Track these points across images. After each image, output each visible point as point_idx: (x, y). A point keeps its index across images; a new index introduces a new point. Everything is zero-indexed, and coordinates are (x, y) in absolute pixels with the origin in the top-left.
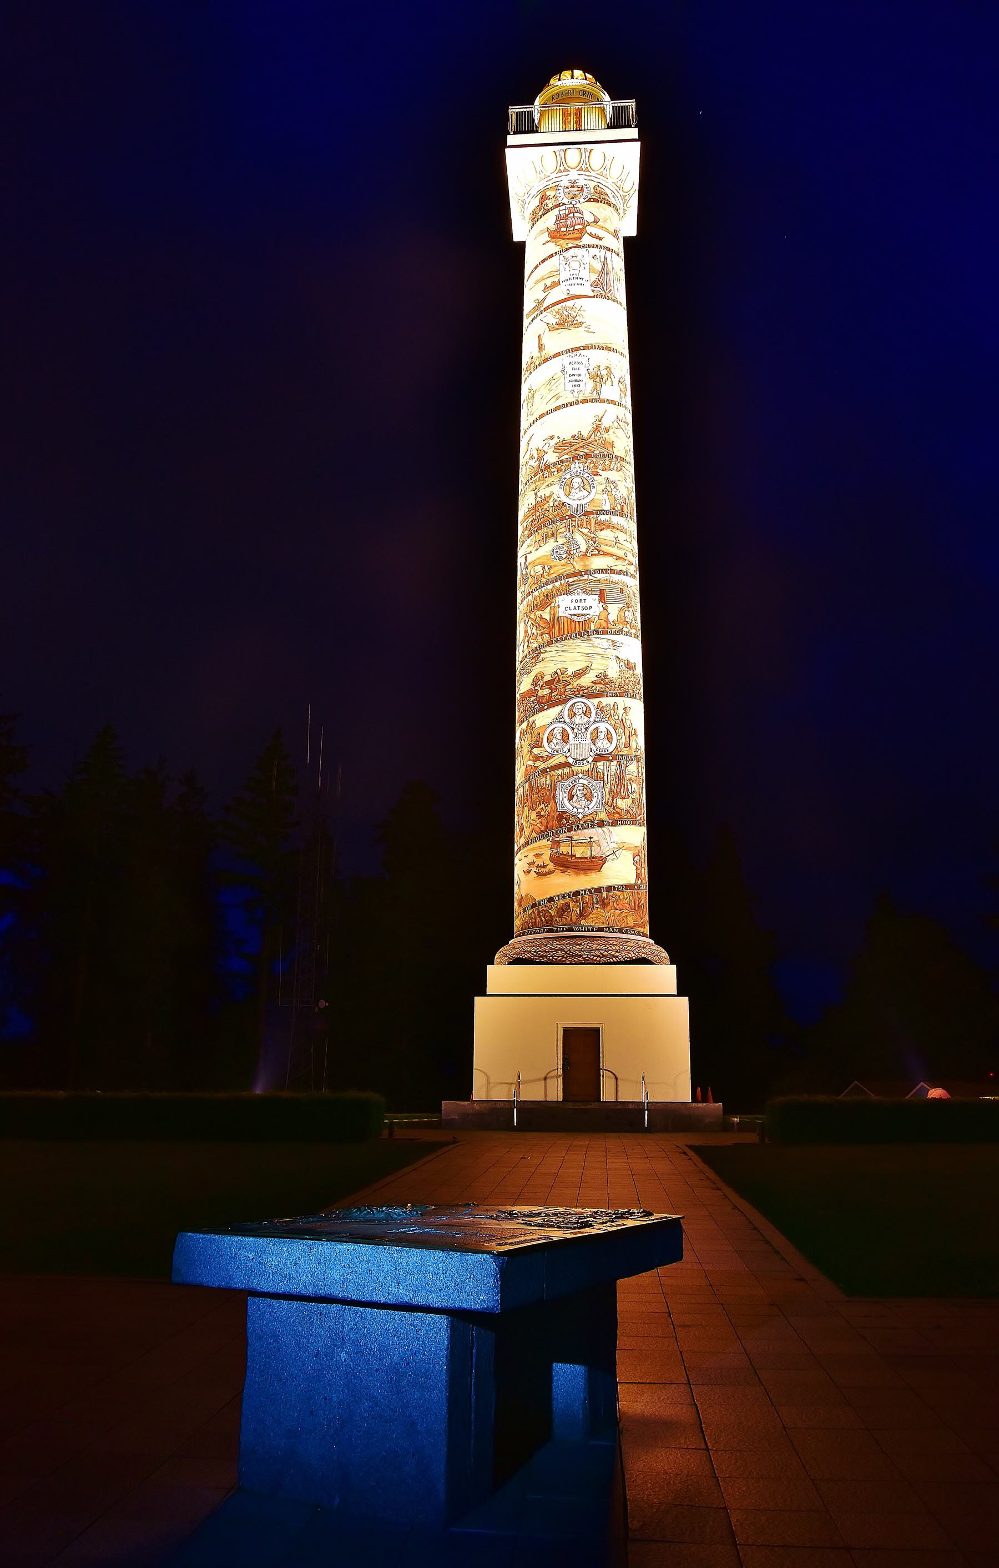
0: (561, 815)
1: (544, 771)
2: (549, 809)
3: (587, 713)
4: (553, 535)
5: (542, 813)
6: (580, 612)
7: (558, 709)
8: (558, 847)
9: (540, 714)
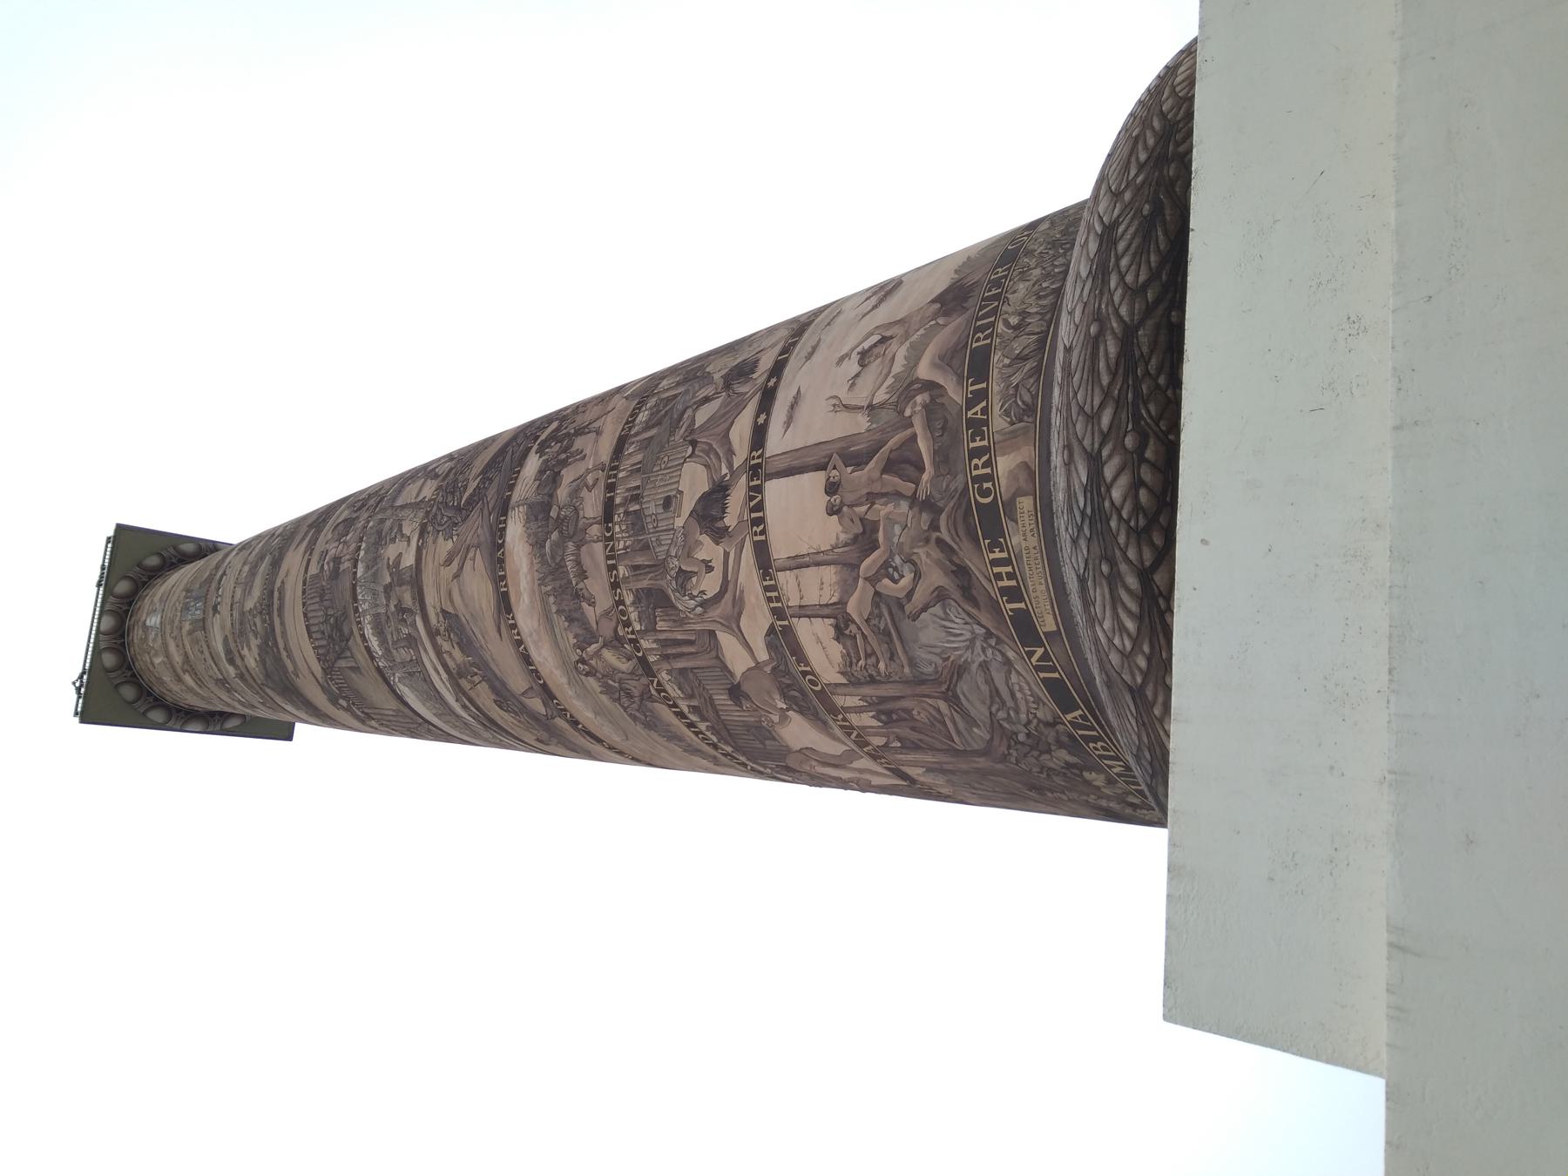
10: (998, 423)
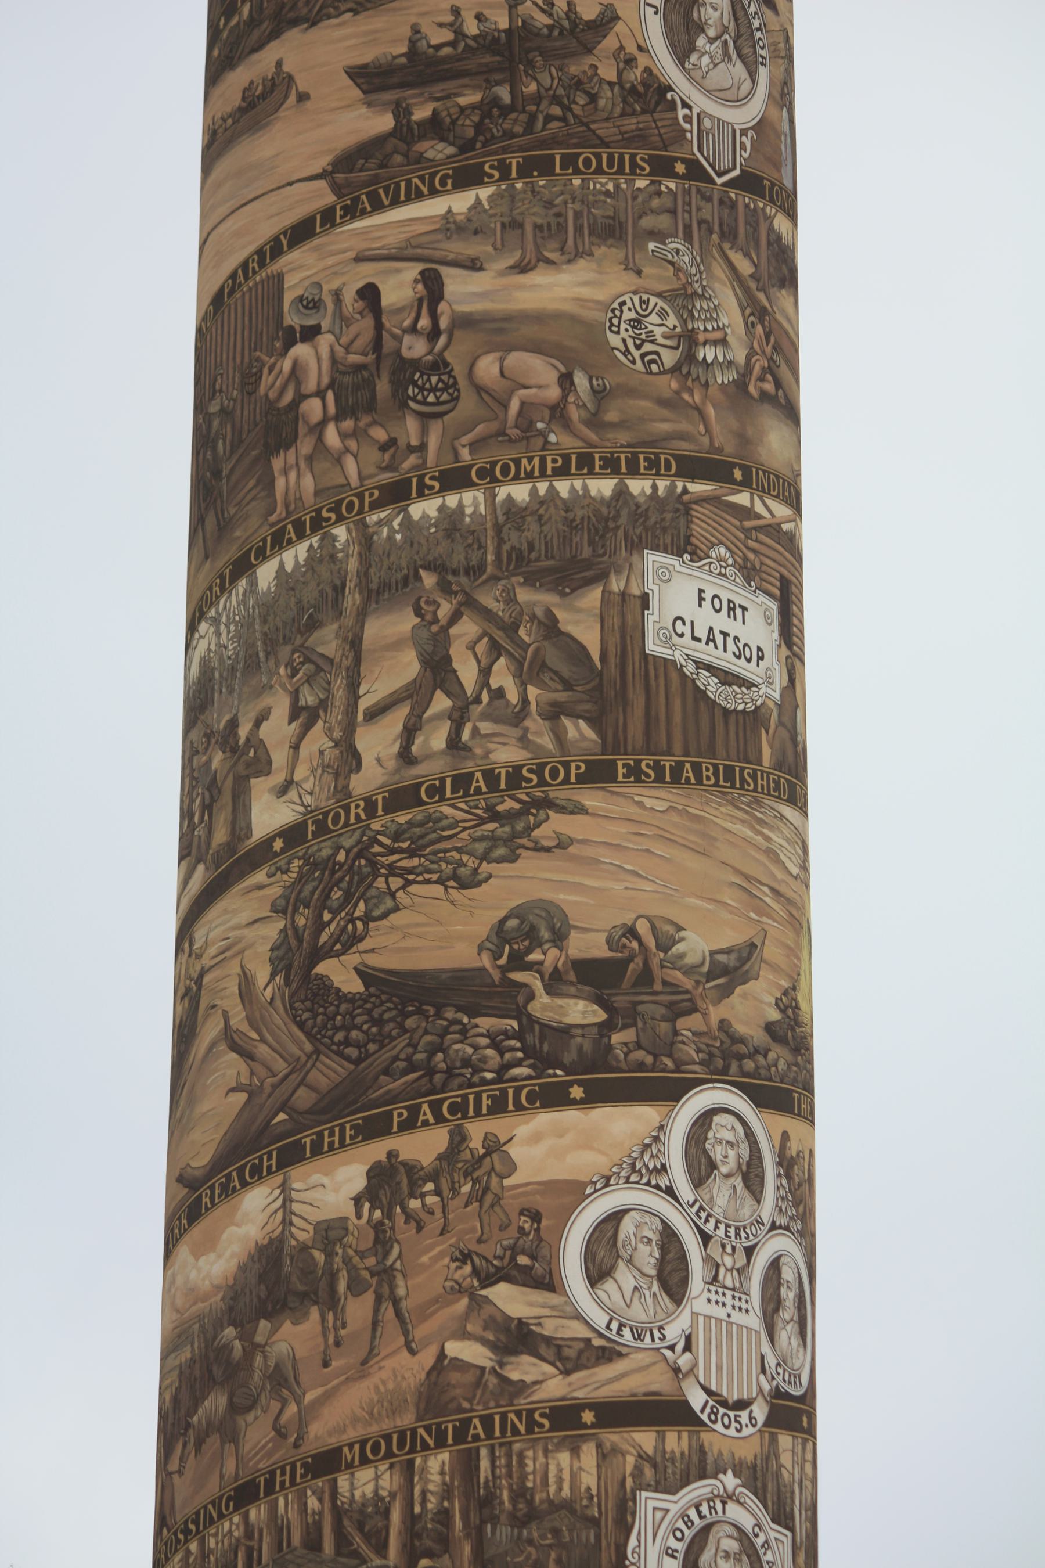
1: (565, 1416)
3: (751, 1177)
4: (612, 231)
6: (725, 660)
9: (545, 1119)
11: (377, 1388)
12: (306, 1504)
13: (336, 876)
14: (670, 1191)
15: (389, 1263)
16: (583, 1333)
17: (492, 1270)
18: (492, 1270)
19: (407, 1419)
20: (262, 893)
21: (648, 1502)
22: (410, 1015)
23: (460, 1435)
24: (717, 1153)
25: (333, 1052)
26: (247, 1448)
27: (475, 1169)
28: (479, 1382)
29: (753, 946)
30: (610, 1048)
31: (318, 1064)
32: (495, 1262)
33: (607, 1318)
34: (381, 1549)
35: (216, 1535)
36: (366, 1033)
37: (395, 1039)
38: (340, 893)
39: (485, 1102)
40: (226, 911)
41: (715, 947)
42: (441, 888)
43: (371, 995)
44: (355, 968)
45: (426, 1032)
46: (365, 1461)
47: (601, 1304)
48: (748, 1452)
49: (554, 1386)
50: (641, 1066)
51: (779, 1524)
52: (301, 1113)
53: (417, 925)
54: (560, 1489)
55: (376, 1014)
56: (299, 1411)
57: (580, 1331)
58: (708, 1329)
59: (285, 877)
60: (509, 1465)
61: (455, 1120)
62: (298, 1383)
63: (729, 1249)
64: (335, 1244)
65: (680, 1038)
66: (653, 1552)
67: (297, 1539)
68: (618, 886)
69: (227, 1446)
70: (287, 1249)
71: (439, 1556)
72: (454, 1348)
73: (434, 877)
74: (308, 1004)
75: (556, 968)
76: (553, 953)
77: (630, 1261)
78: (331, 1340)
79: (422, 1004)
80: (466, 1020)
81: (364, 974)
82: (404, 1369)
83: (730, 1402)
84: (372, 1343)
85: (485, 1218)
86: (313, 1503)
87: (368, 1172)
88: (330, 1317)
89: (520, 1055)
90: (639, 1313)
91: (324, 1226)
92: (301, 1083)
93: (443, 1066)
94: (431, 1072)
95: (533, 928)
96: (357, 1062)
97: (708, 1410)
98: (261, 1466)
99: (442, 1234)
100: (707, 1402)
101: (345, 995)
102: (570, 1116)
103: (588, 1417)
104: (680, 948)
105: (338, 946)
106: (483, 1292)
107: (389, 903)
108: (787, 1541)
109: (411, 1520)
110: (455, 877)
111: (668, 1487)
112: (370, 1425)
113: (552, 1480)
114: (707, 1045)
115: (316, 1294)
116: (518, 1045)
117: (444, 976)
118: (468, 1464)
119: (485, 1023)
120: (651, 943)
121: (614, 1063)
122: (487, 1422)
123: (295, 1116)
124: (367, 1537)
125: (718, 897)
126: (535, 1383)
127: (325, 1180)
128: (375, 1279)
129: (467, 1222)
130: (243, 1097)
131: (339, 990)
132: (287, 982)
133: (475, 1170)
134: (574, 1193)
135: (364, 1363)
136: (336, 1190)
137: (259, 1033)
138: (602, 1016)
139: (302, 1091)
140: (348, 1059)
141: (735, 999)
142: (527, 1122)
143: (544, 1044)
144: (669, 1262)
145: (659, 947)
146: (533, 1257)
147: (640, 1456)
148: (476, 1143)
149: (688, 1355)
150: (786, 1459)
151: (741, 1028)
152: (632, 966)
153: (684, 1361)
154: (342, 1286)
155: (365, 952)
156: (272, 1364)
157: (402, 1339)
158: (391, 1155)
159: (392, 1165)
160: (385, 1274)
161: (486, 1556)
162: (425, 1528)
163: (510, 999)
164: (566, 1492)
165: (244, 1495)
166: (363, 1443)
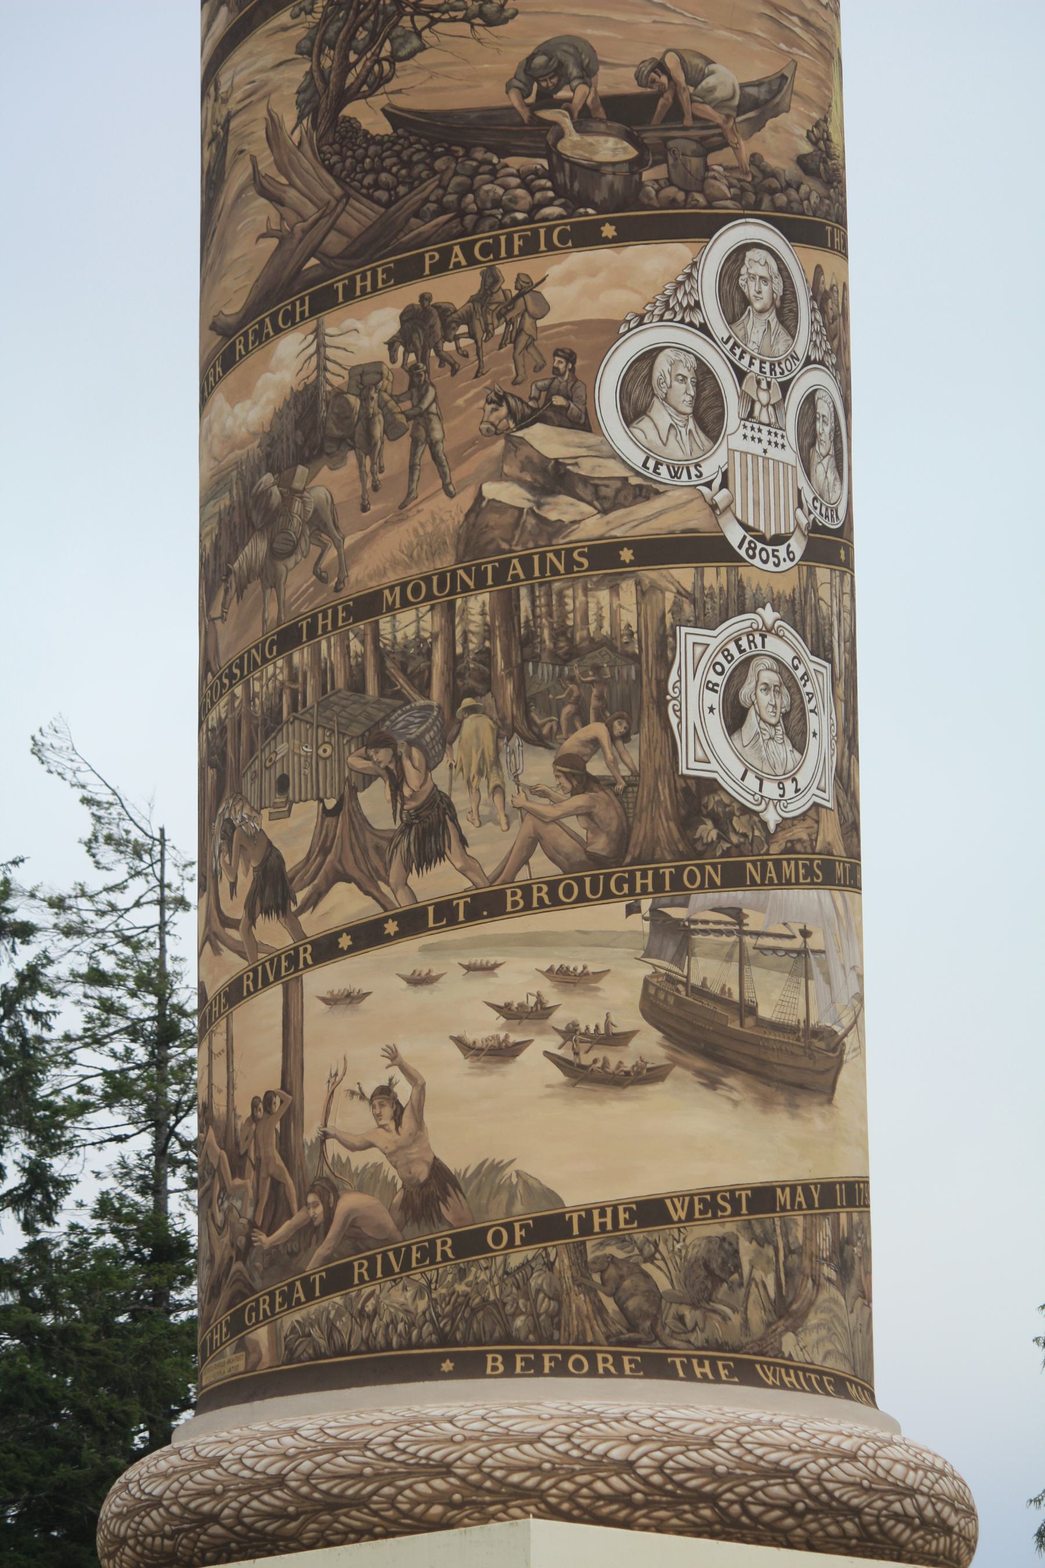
0: (698, 797)
1: (604, 555)
2: (633, 753)
3: (785, 311)
5: (596, 767)
7: (679, 252)
8: (684, 950)
9: (577, 258)
10: (290, 1319)
11: (415, 530)
12: (348, 646)
13: (361, 16)
14: (704, 328)
15: (424, 406)
16: (621, 472)
17: (527, 411)
18: (527, 411)
19: (447, 561)
20: (286, 34)
21: (688, 638)
22: (439, 156)
23: (500, 576)
24: (751, 289)
25: (363, 195)
26: (289, 592)
27: (508, 310)
28: (517, 524)
29: (783, 78)
30: (641, 185)
31: (348, 208)
32: (531, 403)
33: (644, 456)
34: (425, 689)
35: (260, 679)
36: (395, 175)
37: (423, 181)
38: (365, 33)
39: (517, 243)
40: (251, 54)
41: (744, 80)
42: (468, 26)
43: (399, 137)
44: (383, 110)
45: (456, 173)
46: (406, 604)
47: (636, 442)
48: (786, 586)
49: (593, 526)
50: (673, 203)
51: (818, 656)
52: (332, 258)
53: (445, 64)
54: (601, 627)
55: (405, 156)
56: (339, 555)
57: (615, 470)
58: (744, 465)
59: (309, 18)
60: (549, 604)
61: (487, 261)
62: (337, 528)
63: (764, 385)
64: (370, 389)
65: (711, 174)
66: (694, 686)
67: (340, 682)
68: (646, 20)
69: (268, 591)
70: (322, 395)
71: (482, 695)
72: (492, 490)
73: (460, 15)
74: (336, 147)
75: (585, 105)
76: (582, 89)
77: (665, 399)
78: (369, 485)
79: (451, 145)
80: (495, 160)
81: (392, 115)
82: (442, 512)
83: (768, 537)
84: (409, 487)
85: (520, 359)
86: (355, 646)
87: (401, 316)
88: (368, 461)
89: (551, 194)
90: (675, 451)
91: (360, 370)
92: (332, 227)
93: (473, 207)
94: (461, 213)
95: (561, 65)
96: (387, 205)
97: (746, 545)
98: (303, 610)
99: (476, 377)
100: (745, 538)
101: (373, 137)
102: (602, 255)
103: (627, 555)
104: (710, 81)
105: (365, 88)
106: (519, 434)
107: (415, 42)
108: (827, 672)
109: (453, 660)
110: (481, 14)
111: (705, 621)
112: (410, 568)
113: (592, 618)
114: (739, 180)
115: (352, 438)
116: (549, 184)
117: (473, 116)
118: (508, 605)
119: (515, 163)
120: (681, 77)
121: (646, 201)
122: (526, 562)
123: (326, 260)
124: (410, 678)
125: (748, 29)
126: (574, 522)
127: (359, 325)
128: (411, 423)
129: (501, 365)
130: (274, 242)
131: (367, 132)
132: (315, 125)
133: (508, 311)
134: (609, 332)
135: (402, 506)
136: (370, 335)
137: (288, 177)
138: (632, 153)
139: (333, 236)
140: (377, 202)
141: (766, 132)
142: (559, 262)
143: (574, 183)
144: (705, 399)
145: (688, 81)
146: (568, 398)
147: (679, 593)
148: (509, 284)
149: (725, 491)
150: (824, 592)
151: (772, 162)
152: (661, 101)
153: (721, 498)
154: (378, 430)
155: (392, 93)
156: (310, 509)
157: (440, 482)
158: (424, 298)
159: (425, 309)
160: (421, 418)
161: (528, 694)
162: (467, 668)
163: (540, 138)
164: (606, 629)
165: (287, 639)
166: (404, 586)
